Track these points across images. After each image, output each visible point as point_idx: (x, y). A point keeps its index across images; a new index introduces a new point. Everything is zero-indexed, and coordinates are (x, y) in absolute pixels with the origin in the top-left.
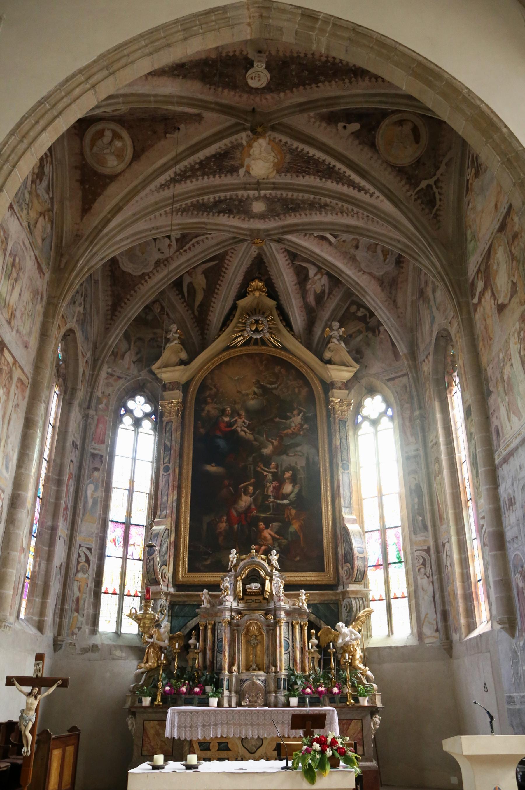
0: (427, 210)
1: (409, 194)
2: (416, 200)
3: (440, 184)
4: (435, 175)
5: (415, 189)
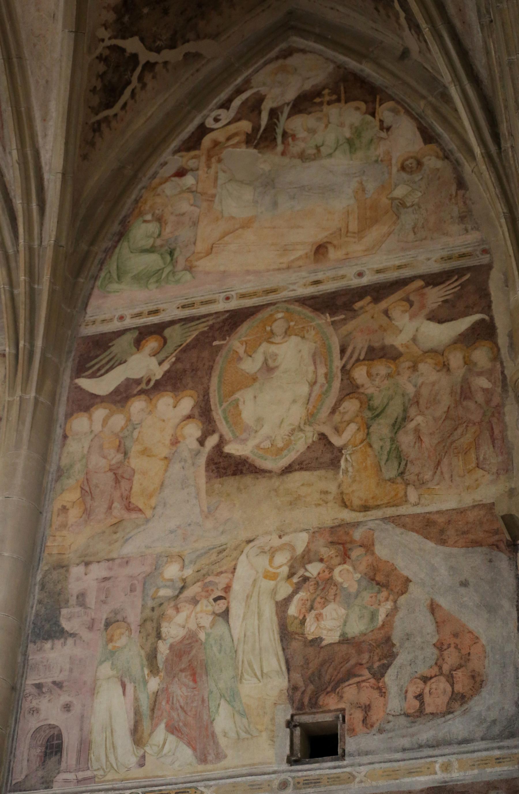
0: (96, 101)
1: (102, 33)
2: (100, 58)
3: (148, 77)
4: (158, 50)
5: (115, 37)
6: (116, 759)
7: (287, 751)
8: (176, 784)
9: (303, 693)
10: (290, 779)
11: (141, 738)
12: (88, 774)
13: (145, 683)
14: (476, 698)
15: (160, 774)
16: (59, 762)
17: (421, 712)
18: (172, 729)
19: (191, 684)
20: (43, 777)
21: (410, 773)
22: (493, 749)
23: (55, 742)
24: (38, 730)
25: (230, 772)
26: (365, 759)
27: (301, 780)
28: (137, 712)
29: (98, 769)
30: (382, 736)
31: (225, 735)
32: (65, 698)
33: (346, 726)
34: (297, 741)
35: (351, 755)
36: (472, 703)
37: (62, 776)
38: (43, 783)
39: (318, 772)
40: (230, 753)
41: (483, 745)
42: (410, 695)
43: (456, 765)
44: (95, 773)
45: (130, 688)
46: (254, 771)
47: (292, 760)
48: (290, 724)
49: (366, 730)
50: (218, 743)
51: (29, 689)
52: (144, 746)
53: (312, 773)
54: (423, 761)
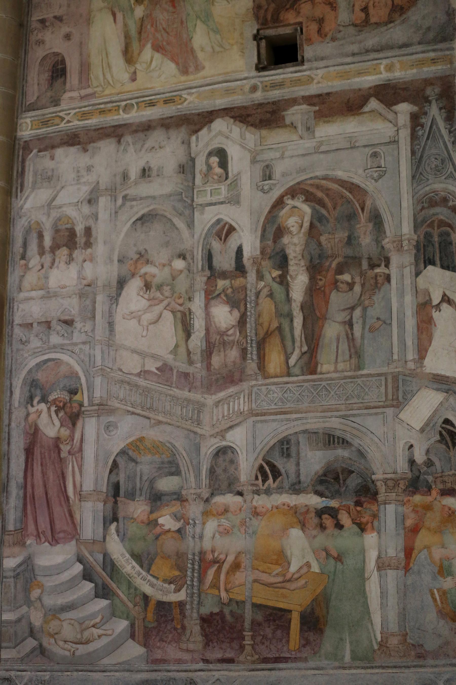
6: (112, 77)
7: (255, 60)
8: (164, 93)
9: (266, 10)
10: (259, 84)
11: (132, 57)
13: (132, 10)
14: (413, 9)
15: (149, 86)
16: (65, 83)
17: (366, 22)
18: (157, 48)
19: (171, 9)
20: (51, 97)
21: (360, 73)
22: (428, 51)
23: (60, 67)
25: (208, 81)
26: (321, 64)
27: (268, 84)
28: (127, 36)
29: (97, 86)
30: (334, 44)
31: (202, 50)
32: (65, 29)
33: (304, 37)
34: (263, 51)
35: (309, 61)
36: (410, 13)
38: (52, 102)
39: (282, 76)
40: (207, 64)
41: (420, 48)
42: (357, 8)
43: (398, 66)
44: (95, 89)
45: (119, 16)
46: (228, 78)
47: (260, 68)
48: (257, 37)
49: (321, 39)
50: (196, 57)
51: (35, 25)
52: (135, 63)
53: (277, 77)
54: (369, 63)
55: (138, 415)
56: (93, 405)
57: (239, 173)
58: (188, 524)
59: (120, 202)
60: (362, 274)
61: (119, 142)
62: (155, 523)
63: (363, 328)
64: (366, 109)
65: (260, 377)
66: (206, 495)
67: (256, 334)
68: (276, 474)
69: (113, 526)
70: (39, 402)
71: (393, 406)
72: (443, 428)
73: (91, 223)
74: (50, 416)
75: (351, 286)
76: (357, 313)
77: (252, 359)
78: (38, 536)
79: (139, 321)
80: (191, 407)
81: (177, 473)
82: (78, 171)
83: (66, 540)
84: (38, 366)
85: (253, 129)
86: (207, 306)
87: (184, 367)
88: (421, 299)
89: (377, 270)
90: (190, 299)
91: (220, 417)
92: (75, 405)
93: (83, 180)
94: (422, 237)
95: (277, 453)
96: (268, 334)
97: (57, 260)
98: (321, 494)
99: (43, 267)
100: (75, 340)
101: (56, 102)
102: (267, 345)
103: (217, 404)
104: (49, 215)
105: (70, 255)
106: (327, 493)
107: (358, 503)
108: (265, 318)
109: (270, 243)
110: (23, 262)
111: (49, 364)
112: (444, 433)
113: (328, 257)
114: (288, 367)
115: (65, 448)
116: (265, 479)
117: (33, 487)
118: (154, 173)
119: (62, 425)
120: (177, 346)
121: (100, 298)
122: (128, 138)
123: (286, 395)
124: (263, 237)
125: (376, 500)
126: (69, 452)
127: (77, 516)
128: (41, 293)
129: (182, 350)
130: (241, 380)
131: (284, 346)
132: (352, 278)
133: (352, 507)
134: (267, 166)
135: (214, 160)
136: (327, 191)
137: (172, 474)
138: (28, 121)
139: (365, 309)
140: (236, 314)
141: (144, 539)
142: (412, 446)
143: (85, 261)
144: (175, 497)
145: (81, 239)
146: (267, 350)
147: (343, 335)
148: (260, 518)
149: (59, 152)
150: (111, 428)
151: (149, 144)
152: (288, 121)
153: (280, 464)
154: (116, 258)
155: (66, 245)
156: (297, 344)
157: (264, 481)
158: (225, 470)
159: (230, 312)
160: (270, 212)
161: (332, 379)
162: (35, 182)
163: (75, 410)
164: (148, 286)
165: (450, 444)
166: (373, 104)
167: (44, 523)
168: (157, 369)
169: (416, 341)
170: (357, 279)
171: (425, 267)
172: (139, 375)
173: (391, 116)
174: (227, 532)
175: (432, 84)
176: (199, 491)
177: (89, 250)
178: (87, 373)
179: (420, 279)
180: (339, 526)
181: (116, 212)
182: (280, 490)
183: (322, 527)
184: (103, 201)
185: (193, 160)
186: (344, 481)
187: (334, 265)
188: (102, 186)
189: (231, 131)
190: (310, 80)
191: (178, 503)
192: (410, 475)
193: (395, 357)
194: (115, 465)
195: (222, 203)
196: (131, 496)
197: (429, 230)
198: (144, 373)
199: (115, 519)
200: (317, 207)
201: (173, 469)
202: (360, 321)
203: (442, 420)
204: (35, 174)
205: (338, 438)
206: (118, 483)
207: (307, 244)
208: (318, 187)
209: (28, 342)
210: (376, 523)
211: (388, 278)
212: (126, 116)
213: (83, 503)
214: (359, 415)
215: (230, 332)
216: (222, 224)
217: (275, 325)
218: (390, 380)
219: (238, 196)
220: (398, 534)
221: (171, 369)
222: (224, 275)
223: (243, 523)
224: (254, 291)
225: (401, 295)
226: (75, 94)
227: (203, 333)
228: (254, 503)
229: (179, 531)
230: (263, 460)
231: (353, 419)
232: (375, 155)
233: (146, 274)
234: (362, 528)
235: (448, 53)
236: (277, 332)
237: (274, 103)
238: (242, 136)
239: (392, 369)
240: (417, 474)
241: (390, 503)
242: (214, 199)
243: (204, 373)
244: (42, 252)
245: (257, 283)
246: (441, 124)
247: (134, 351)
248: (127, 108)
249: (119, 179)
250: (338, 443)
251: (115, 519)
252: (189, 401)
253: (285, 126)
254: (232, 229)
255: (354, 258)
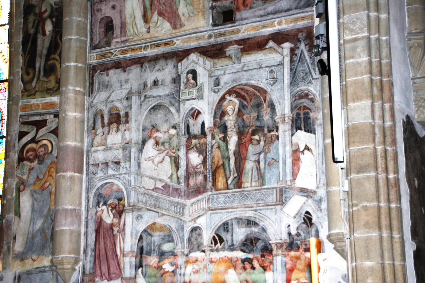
6: (137, 30)
8: (164, 40)
10: (213, 34)
11: (147, 19)
12: (126, 38)
15: (157, 35)
16: (113, 34)
18: (161, 14)
20: (106, 42)
21: (264, 27)
22: (300, 13)
24: (102, 19)
25: (187, 32)
27: (217, 34)
28: (145, 8)
29: (130, 36)
30: (252, 10)
35: (238, 20)
37: (115, 40)
38: (106, 44)
39: (224, 29)
40: (186, 23)
41: (296, 11)
43: (284, 22)
44: (129, 37)
46: (197, 31)
49: (244, 8)
50: (180, 19)
52: (149, 23)
53: (222, 30)
54: (269, 21)
55: (153, 211)
56: (130, 206)
57: (203, 83)
58: (178, 268)
59: (143, 98)
60: (265, 135)
61: (142, 66)
62: (159, 268)
63: (265, 164)
64: (267, 47)
65: (213, 190)
66: (186, 252)
67: (211, 168)
68: (222, 240)
69: (140, 270)
70: (102, 205)
71: (280, 205)
72: (305, 216)
73: (128, 110)
74: (108, 212)
75: (259, 141)
76: (262, 156)
77: (210, 181)
78: (102, 276)
79: (153, 162)
80: (179, 206)
81: (172, 241)
82: (121, 83)
83: (116, 278)
84: (102, 186)
85: (210, 59)
86: (187, 153)
87: (176, 186)
88: (294, 148)
89: (272, 133)
90: (179, 150)
91: (194, 211)
92: (121, 206)
93: (124, 87)
94: (295, 115)
95: (222, 229)
96: (217, 168)
97: (111, 130)
98: (244, 251)
99: (104, 134)
100: (121, 172)
101: (109, 44)
102: (217, 173)
103: (192, 204)
104: (106, 106)
105: (118, 127)
106: (247, 251)
107: (263, 256)
108: (216, 160)
109: (218, 120)
110: (93, 131)
111: (108, 185)
112: (306, 218)
113: (247, 127)
114: (227, 185)
115: (116, 229)
116: (216, 243)
117: (99, 250)
118: (160, 83)
119: (114, 217)
120: (172, 175)
121: (133, 150)
122: (147, 65)
123: (226, 199)
124: (215, 117)
125: (272, 254)
126: (118, 231)
127: (122, 265)
128: (103, 147)
129: (175, 176)
130: (204, 192)
131: (225, 174)
132: (260, 138)
133: (259, 258)
134: (217, 79)
135: (190, 76)
136: (247, 91)
137: (169, 241)
138: (95, 54)
139: (266, 154)
140: (202, 157)
141: (155, 276)
142: (289, 226)
143: (125, 130)
144: (171, 253)
145: (123, 119)
146: (217, 176)
147: (255, 168)
148: (213, 264)
149: (111, 72)
150: (139, 218)
151: (157, 67)
152: (227, 54)
153: (223, 235)
154: (141, 129)
155: (115, 122)
156: (232, 173)
157: (216, 244)
158: (196, 239)
159: (199, 156)
160: (218, 103)
161: (250, 191)
162: (99, 88)
163: (121, 209)
164: (157, 143)
165: (309, 225)
166: (271, 44)
167: (104, 269)
168: (162, 187)
169: (291, 170)
170: (262, 138)
171: (296, 131)
172: (153, 190)
173: (280, 50)
174: (197, 272)
175: (302, 32)
176: (183, 250)
177: (127, 125)
178: (126, 189)
179: (294, 137)
180: (253, 268)
181: (141, 104)
182: (223, 249)
183: (245, 269)
184: (134, 98)
185: (179, 76)
186: (256, 244)
187: (250, 131)
188: (134, 91)
189: (198, 60)
190: (239, 31)
191: (173, 257)
192: (288, 241)
193: (281, 179)
194: (141, 238)
195: (194, 99)
196: (149, 253)
197: (298, 111)
198: (156, 189)
199: (141, 266)
200: (242, 100)
201: (170, 239)
202: (264, 160)
203: (304, 212)
204: (99, 84)
205: (252, 221)
206: (142, 247)
207: (237, 120)
208: (242, 89)
209: (96, 173)
210: (271, 267)
211: (277, 137)
212: (145, 52)
213: (125, 258)
214: (263, 209)
215: (199, 167)
216: (194, 110)
217: (221, 163)
218: (278, 191)
219: (202, 95)
220: (283, 272)
221: (169, 187)
222: (195, 137)
223: (205, 267)
224: (210, 145)
225: (284, 146)
226: (118, 40)
227: (185, 168)
228: (211, 256)
229: (173, 272)
230: (215, 233)
231: (259, 211)
232: (272, 72)
233: (156, 137)
234: (265, 269)
235: (310, 13)
236: (222, 167)
237: (220, 44)
238: (204, 63)
239: (280, 185)
240: (292, 240)
241: (278, 256)
242: (190, 97)
243: (186, 188)
244: (103, 126)
245: (212, 141)
246: (306, 53)
247: (151, 178)
248: (146, 48)
249: (142, 86)
250: (252, 224)
251: (141, 266)
252: (178, 203)
253: (226, 57)
254: (199, 113)
255: (260, 127)
